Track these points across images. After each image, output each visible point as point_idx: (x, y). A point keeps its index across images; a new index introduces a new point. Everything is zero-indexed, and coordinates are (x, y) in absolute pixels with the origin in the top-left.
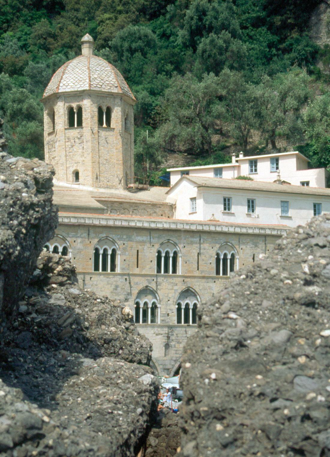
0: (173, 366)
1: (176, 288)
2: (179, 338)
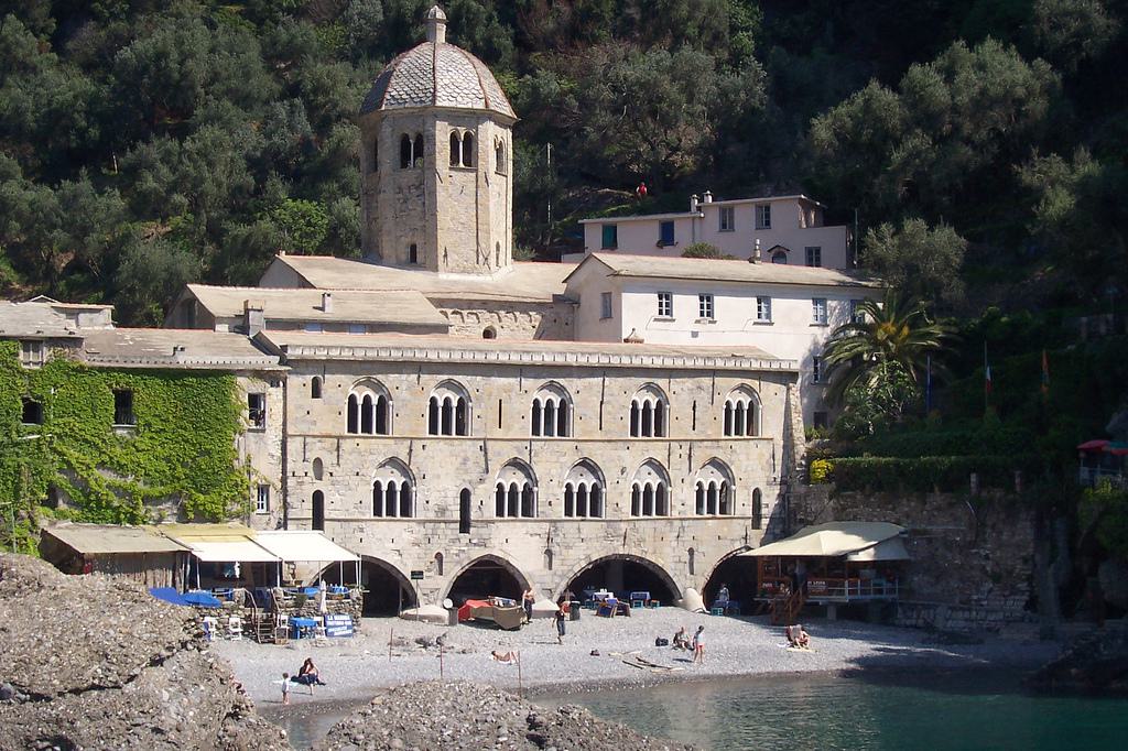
0: (558, 584)
1: (563, 459)
2: (568, 541)
